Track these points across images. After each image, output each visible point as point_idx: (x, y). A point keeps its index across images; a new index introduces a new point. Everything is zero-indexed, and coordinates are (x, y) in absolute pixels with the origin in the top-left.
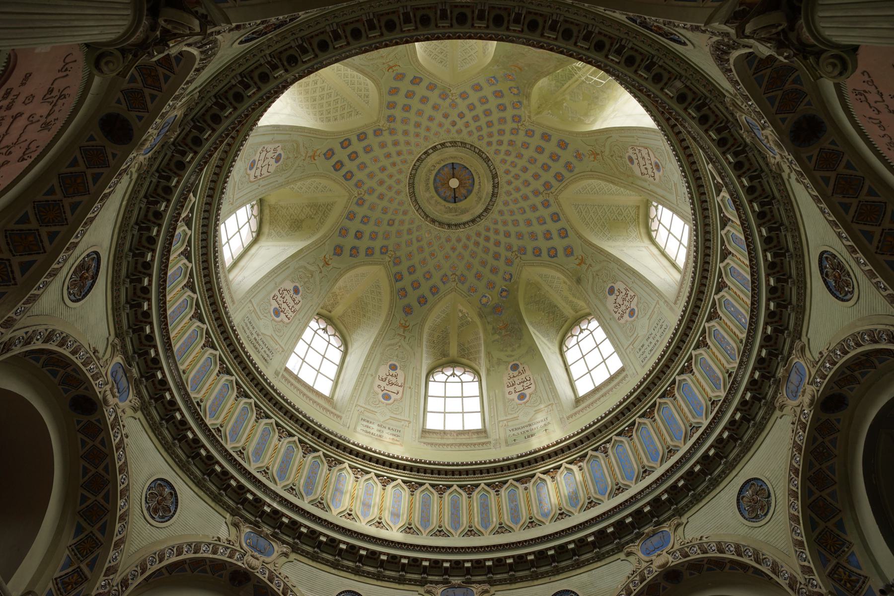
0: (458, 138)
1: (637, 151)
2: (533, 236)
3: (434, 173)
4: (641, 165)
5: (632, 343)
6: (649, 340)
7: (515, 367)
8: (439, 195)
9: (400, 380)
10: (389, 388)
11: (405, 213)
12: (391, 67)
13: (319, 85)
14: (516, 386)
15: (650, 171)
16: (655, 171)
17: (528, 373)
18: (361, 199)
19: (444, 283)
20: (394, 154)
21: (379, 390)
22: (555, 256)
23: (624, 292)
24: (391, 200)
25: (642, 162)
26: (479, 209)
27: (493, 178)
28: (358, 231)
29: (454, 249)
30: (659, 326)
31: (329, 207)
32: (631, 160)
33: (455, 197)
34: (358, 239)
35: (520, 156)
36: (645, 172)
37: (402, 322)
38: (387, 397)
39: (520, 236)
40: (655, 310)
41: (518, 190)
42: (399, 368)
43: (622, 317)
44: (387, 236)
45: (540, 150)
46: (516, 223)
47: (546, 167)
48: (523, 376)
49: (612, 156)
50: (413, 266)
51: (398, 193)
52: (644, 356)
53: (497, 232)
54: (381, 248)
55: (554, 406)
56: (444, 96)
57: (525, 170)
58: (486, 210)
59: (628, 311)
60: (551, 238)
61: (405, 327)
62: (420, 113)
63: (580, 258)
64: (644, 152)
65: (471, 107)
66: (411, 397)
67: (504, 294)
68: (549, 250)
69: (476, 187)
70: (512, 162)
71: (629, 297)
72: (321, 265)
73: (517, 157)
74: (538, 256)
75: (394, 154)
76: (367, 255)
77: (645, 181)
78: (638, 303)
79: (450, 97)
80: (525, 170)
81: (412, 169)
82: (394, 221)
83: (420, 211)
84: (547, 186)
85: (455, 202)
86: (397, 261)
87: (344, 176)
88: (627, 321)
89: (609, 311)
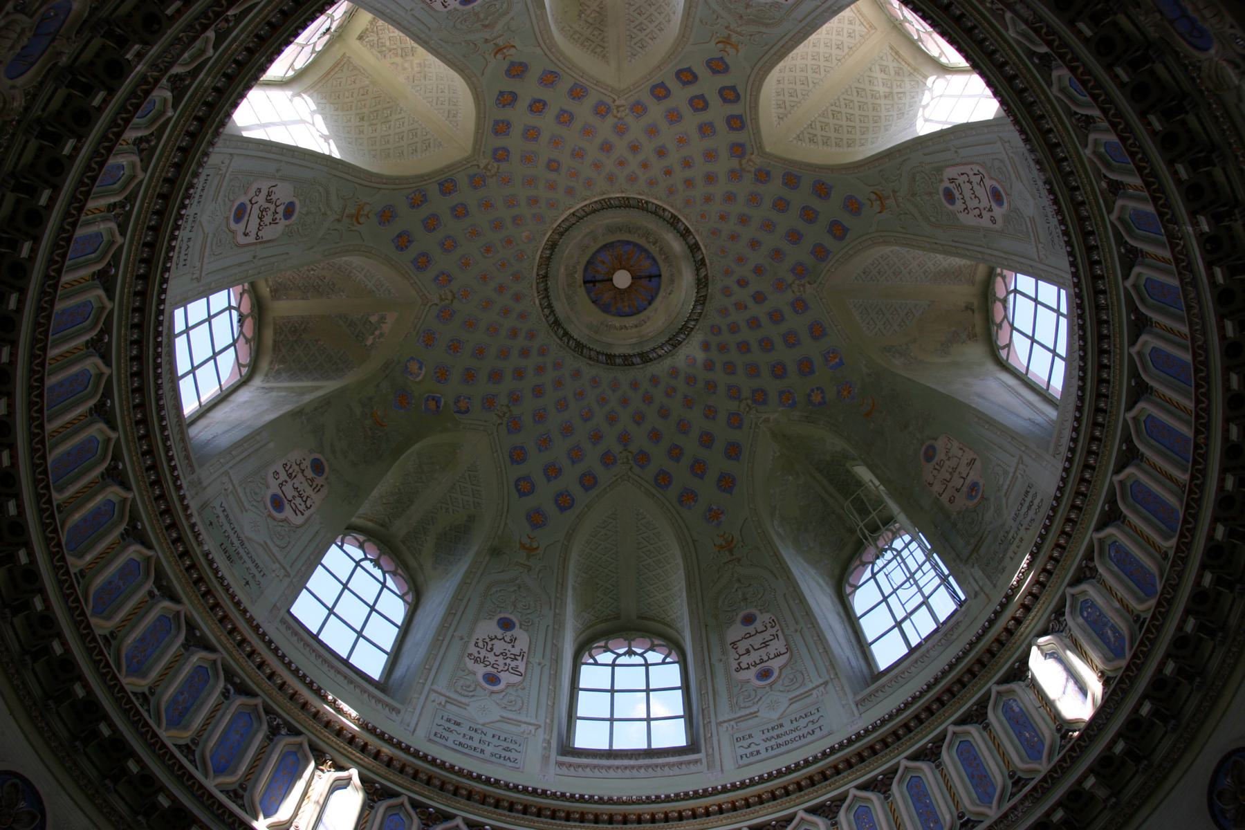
0: (714, 289)
1: (773, 631)
2: (545, 443)
3: (642, 242)
4: (750, 641)
5: (449, 700)
6: (473, 734)
7: (318, 467)
8: (598, 251)
9: (268, 233)
10: (256, 212)
11: (570, 191)
12: (880, 198)
13: (835, 52)
14: (290, 483)
15: (745, 660)
16: (754, 670)
17: (316, 499)
18: (608, 110)
19: (437, 278)
20: (688, 173)
21: (251, 193)
22: (522, 494)
23: (516, 651)
24: (597, 166)
25: (757, 641)
26: (579, 331)
27: (641, 355)
28: (545, 104)
29: (501, 289)
30: (505, 745)
31: (599, 50)
32: (749, 620)
33: (594, 282)
34: (530, 106)
35: (688, 403)
36: (742, 651)
37: (367, 209)
38: (240, 214)
39: (540, 416)
40: (524, 726)
41: (625, 402)
42: (287, 222)
43: (476, 660)
44: (527, 159)
45: (707, 440)
46: (562, 405)
47: (675, 453)
48: (309, 491)
49: (739, 581)
50: (467, 214)
51: (611, 178)
52: (445, 734)
53: (540, 369)
54: (505, 150)
55: (286, 581)
56: (800, 271)
57: (664, 413)
58: (579, 347)
59: (489, 669)
60: (549, 480)
61: (356, 217)
62: (768, 226)
63: (535, 545)
64: (778, 645)
65: (776, 317)
66: (240, 265)
67: (432, 405)
68: (526, 478)
69: (617, 321)
70: (674, 389)
71: (513, 664)
72: (500, 42)
73: (686, 397)
74: (511, 457)
75: (688, 173)
76: (496, 123)
77: (724, 652)
78: (513, 685)
79: (798, 282)
80: (664, 413)
81: (657, 206)
82: (556, 170)
83: (573, 220)
84: (642, 458)
85: (585, 282)
86: (477, 181)
87: (662, 85)
88: (475, 674)
89: (472, 630)
